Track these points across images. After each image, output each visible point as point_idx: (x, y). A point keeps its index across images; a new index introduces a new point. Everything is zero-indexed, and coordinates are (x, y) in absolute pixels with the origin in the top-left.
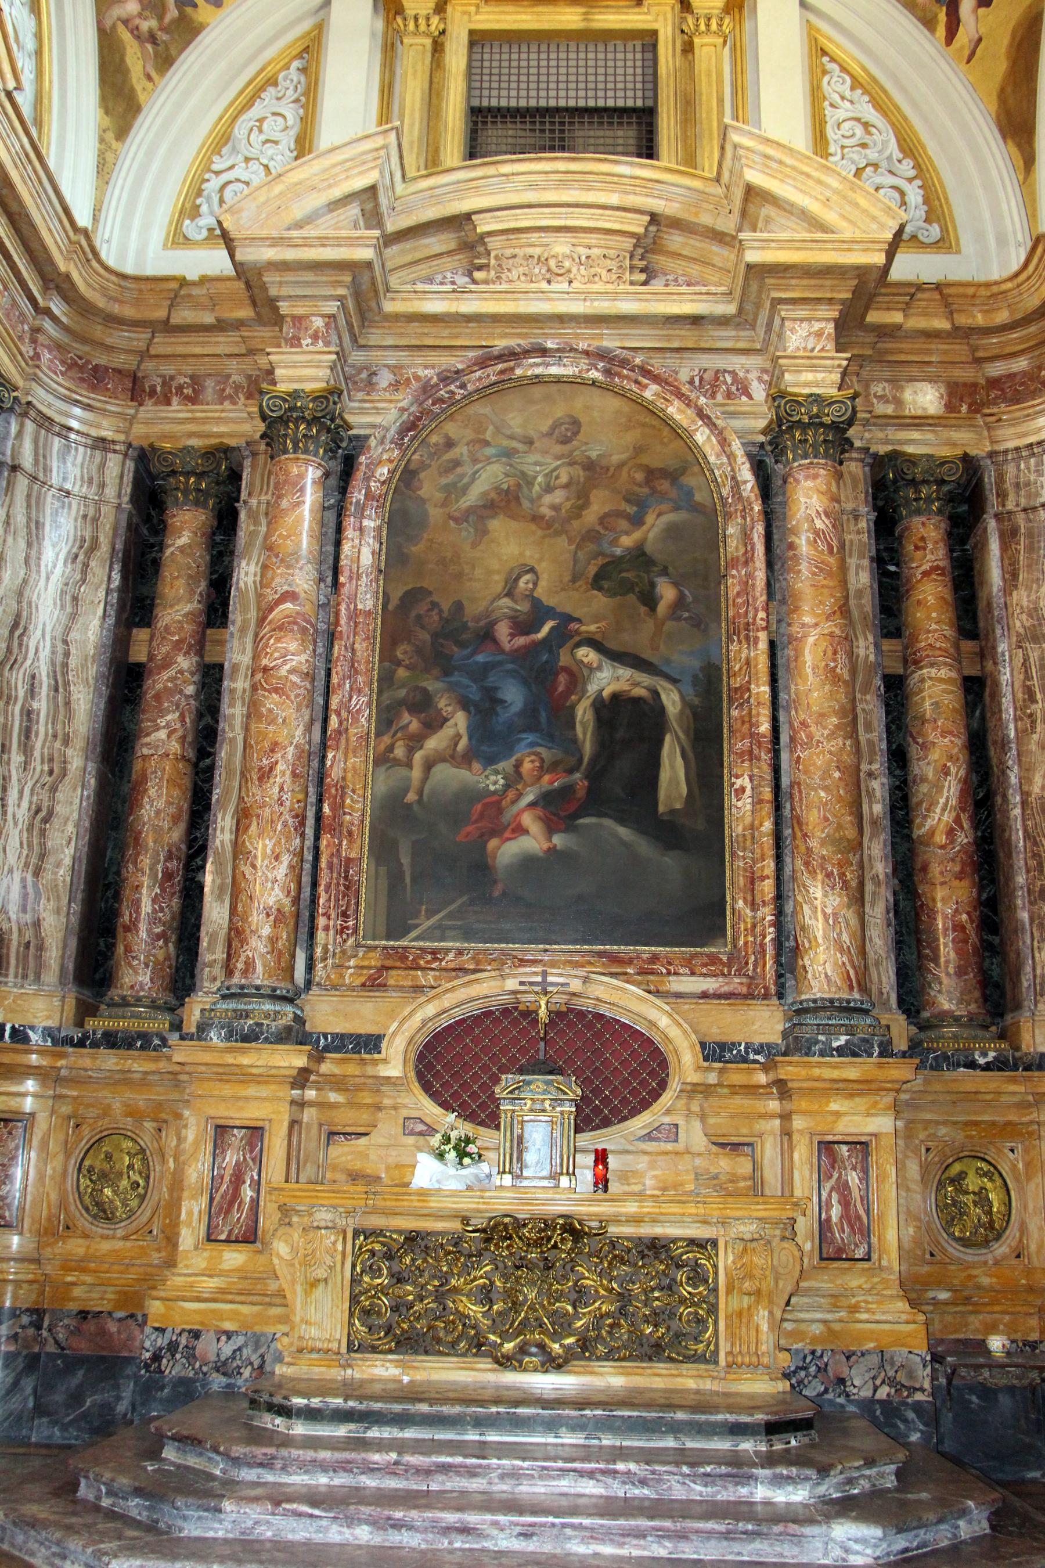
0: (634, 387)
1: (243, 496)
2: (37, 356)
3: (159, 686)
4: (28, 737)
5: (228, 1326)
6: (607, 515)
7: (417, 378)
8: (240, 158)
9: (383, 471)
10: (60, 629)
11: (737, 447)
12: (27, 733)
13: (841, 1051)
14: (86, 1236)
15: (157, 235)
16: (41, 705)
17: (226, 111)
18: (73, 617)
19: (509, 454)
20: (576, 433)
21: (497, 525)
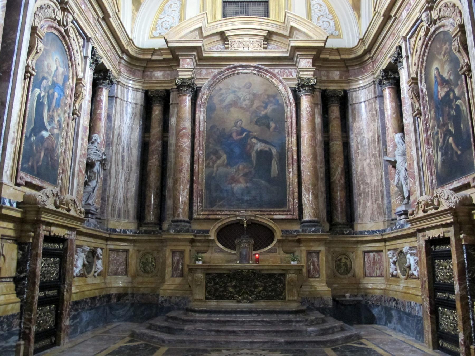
0: (264, 75)
1: (171, 102)
2: (120, 69)
3: (153, 149)
4: (123, 162)
5: (178, 295)
6: (259, 106)
7: (212, 72)
8: (166, 15)
9: (205, 97)
10: (129, 135)
11: (289, 90)
12: (123, 161)
13: (312, 231)
14: (143, 277)
15: (147, 36)
16: (125, 154)
17: (162, 3)
18: (132, 132)
19: (234, 92)
20: (251, 86)
21: (232, 109)
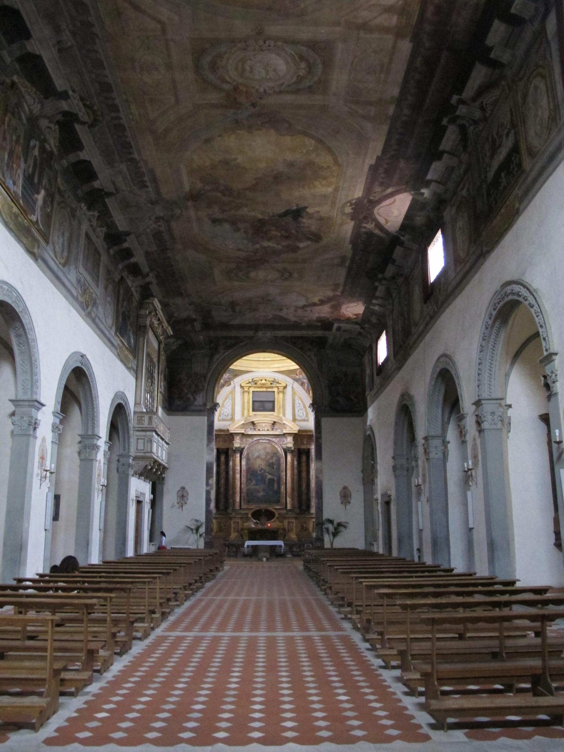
19: (258, 451)
